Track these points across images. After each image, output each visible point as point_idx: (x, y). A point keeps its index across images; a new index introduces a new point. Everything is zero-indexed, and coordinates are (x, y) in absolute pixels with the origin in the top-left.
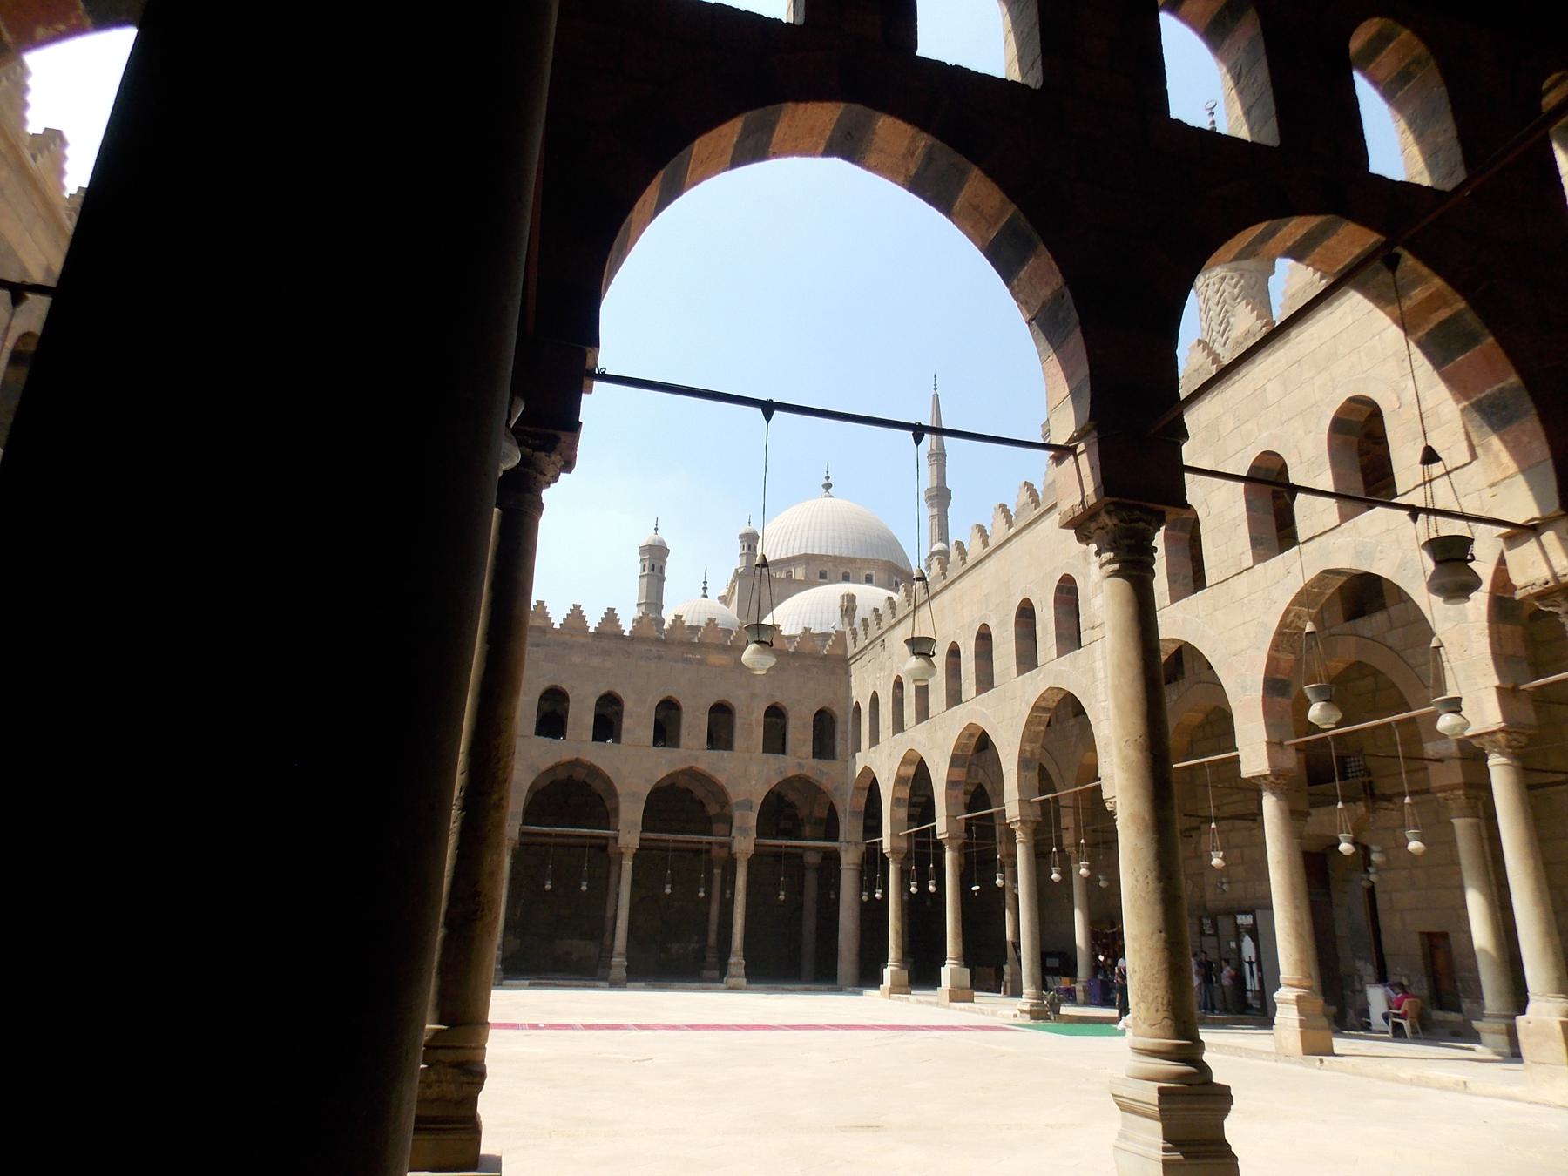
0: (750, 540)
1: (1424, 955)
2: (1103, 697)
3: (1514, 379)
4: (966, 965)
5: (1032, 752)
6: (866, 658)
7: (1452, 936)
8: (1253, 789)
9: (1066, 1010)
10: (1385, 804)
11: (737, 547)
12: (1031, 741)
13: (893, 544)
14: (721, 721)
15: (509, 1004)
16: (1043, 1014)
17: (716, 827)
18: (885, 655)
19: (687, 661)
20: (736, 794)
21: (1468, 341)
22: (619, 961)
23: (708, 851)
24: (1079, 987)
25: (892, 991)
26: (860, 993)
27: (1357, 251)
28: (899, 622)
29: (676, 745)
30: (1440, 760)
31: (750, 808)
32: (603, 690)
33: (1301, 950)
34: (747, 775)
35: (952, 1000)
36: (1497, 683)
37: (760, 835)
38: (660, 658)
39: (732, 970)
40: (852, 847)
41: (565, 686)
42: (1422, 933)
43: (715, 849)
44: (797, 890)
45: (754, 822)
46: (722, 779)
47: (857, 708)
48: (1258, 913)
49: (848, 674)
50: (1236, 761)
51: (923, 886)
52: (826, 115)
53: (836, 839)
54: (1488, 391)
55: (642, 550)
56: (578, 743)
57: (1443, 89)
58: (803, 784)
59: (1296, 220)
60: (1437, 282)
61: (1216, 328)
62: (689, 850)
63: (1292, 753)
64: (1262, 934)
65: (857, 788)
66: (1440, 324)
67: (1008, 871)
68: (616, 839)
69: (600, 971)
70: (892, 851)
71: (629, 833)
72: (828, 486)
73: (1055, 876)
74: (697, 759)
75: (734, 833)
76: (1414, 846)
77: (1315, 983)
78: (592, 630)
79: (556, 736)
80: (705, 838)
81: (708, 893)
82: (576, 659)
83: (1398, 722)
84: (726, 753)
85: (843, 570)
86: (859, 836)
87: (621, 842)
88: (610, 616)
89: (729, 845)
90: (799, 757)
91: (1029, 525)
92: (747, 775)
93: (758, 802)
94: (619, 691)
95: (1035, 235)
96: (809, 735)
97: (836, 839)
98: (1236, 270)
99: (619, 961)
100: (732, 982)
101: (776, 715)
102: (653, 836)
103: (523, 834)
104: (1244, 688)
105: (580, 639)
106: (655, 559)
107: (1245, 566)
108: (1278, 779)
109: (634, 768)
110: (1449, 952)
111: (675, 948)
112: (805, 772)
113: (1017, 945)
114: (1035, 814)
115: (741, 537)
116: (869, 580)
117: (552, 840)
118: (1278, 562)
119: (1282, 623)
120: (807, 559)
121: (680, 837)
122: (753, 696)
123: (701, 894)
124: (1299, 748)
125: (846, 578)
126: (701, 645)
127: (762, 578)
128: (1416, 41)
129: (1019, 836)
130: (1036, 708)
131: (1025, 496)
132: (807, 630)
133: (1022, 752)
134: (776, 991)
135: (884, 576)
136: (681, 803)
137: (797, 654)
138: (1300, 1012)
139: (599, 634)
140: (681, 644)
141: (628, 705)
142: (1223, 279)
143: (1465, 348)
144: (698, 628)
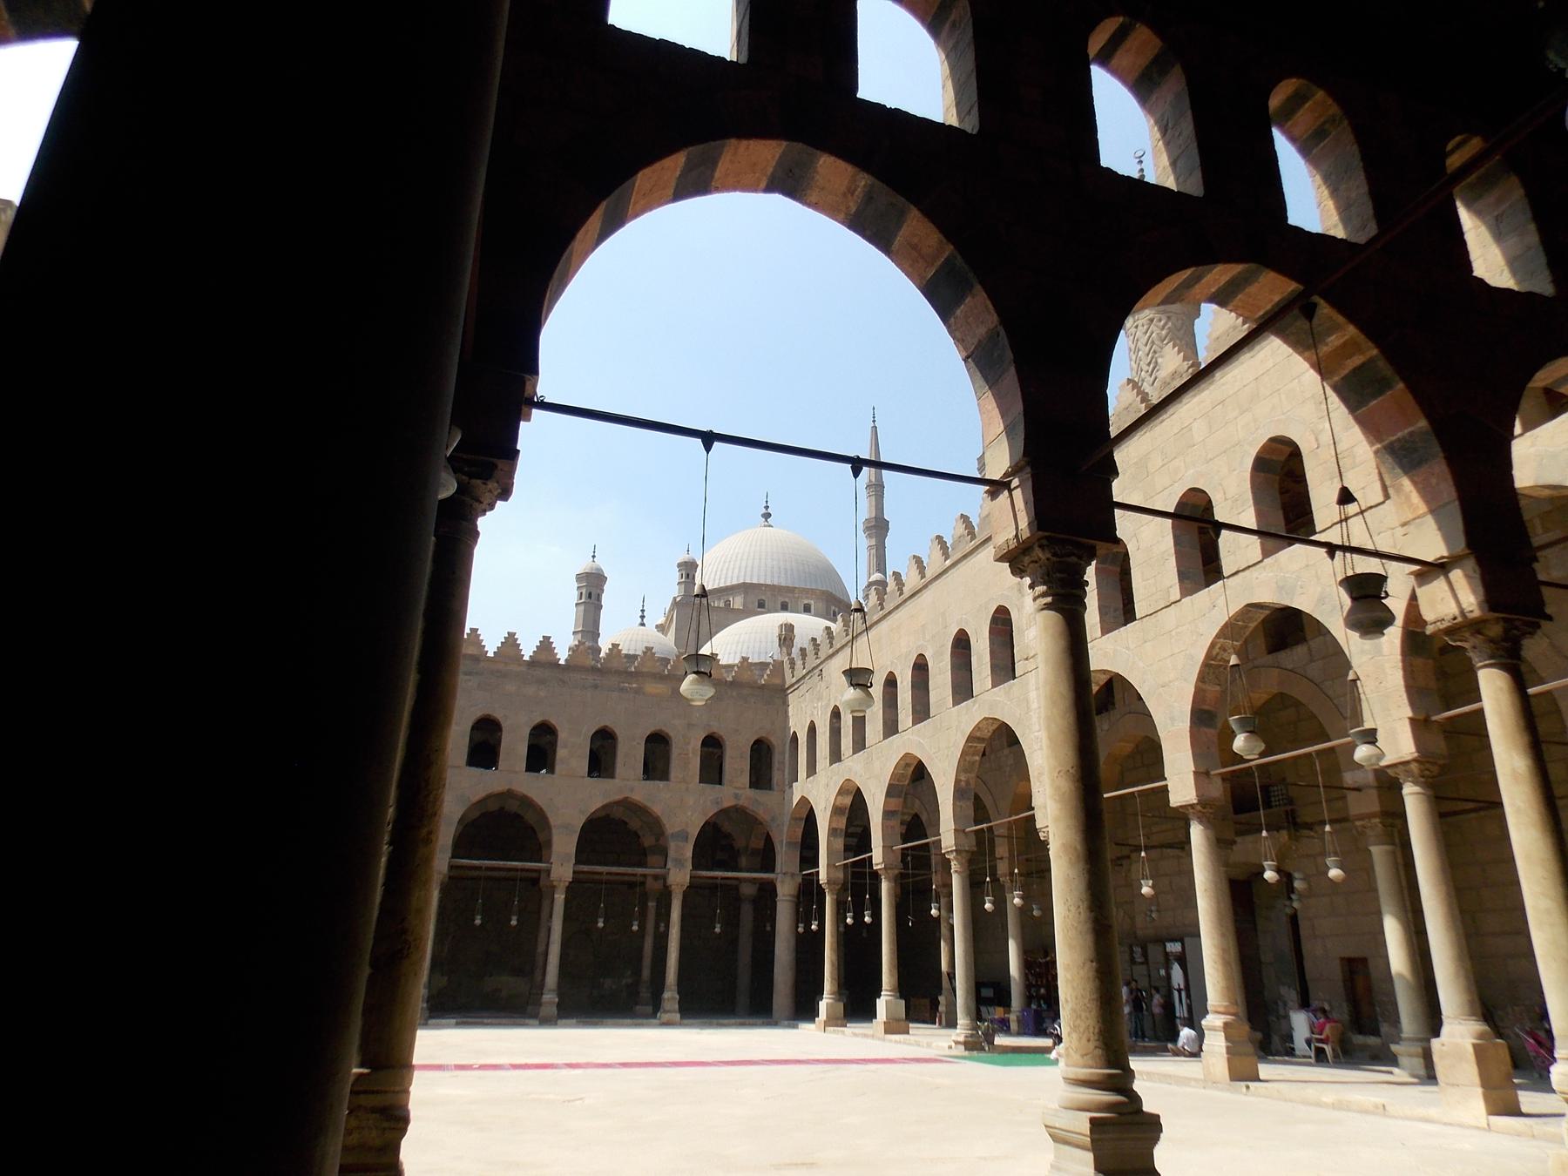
0: (688, 569)
1: (1344, 981)
3: (1423, 423)
4: (901, 997)
5: (968, 783)
6: (803, 688)
7: (1372, 964)
8: (1181, 817)
9: (1000, 1040)
10: (1306, 832)
11: (675, 576)
12: (966, 771)
13: (830, 573)
14: (657, 751)
15: (435, 1045)
16: (978, 1045)
17: (652, 859)
18: (823, 684)
19: (622, 690)
20: (671, 826)
21: (1382, 386)
22: (550, 997)
23: (643, 884)
24: (1013, 1017)
25: (827, 1024)
26: (795, 1027)
27: (1277, 298)
28: (837, 651)
29: (612, 776)
30: (1358, 789)
31: (686, 839)
32: (538, 719)
33: (1228, 977)
34: (683, 805)
35: (887, 1032)
36: (1410, 714)
37: (696, 866)
38: (596, 687)
39: (666, 1005)
40: (788, 879)
41: (498, 715)
42: (1342, 959)
43: (650, 881)
44: (732, 922)
45: (689, 854)
46: (657, 809)
47: (795, 738)
48: (1187, 940)
49: (786, 704)
50: (1165, 789)
51: (858, 917)
52: (768, 152)
53: (773, 871)
54: (1400, 435)
55: (579, 578)
56: (511, 773)
57: (1355, 147)
58: (739, 814)
59: (1220, 268)
60: (1352, 330)
61: (1145, 368)
62: (623, 883)
63: (1219, 781)
64: (1190, 962)
65: (795, 819)
66: (1355, 370)
67: (943, 901)
68: (548, 872)
69: (530, 1008)
70: (829, 882)
71: (562, 866)
72: (767, 516)
73: (988, 906)
74: (632, 790)
75: (669, 865)
76: (1334, 873)
77: (1241, 1010)
78: (526, 658)
79: (488, 767)
80: (640, 870)
81: (642, 927)
82: (510, 687)
83: (1318, 752)
84: (662, 784)
85: (781, 599)
87: (553, 875)
88: (546, 644)
89: (664, 878)
90: (736, 787)
91: (965, 557)
92: (683, 805)
93: (694, 832)
95: (971, 275)
96: (746, 765)
97: (773, 871)
98: (1164, 312)
99: (550, 997)
100: (666, 1017)
101: (712, 744)
102: (586, 868)
103: (451, 867)
104: (1172, 719)
105: (514, 667)
106: (592, 586)
107: (1173, 599)
108: (1205, 809)
109: (568, 799)
110: (1367, 976)
111: (608, 983)
112: (742, 802)
113: (952, 976)
114: (970, 844)
115: (679, 565)
116: (807, 609)
117: (482, 874)
118: (1204, 595)
119: (1209, 656)
120: (745, 588)
121: (614, 869)
123: (635, 928)
124: (1224, 777)
125: (784, 608)
126: (637, 674)
127: (700, 607)
128: (1330, 101)
129: (954, 866)
130: (971, 738)
131: (961, 529)
132: (745, 659)
133: (957, 782)
134: (710, 1026)
135: (821, 606)
136: (615, 836)
137: (734, 684)
138: (1227, 1039)
139: (533, 662)
140: (618, 672)
143: (1381, 392)
144: (635, 657)
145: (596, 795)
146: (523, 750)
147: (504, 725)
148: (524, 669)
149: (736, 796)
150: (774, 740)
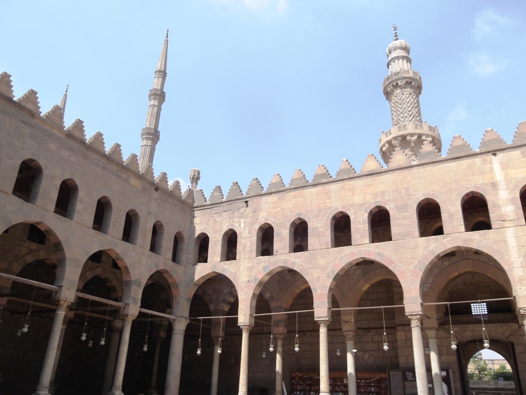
2: (517, 256)
18: (248, 209)
29: (105, 232)
32: (67, 177)
34: (140, 264)
38: (104, 168)
41: (42, 162)
45: (140, 296)
82: (53, 146)
86: (186, 314)
93: (144, 281)
94: (77, 181)
101: (157, 230)
102: (81, 295)
109: (77, 240)
122: (149, 213)
123: (103, 343)
139: (69, 135)
141: (81, 194)
142: (411, 94)
145: (96, 242)
146: (55, 195)
147: (46, 172)
148: (63, 136)
149: (166, 264)
150: (185, 235)
